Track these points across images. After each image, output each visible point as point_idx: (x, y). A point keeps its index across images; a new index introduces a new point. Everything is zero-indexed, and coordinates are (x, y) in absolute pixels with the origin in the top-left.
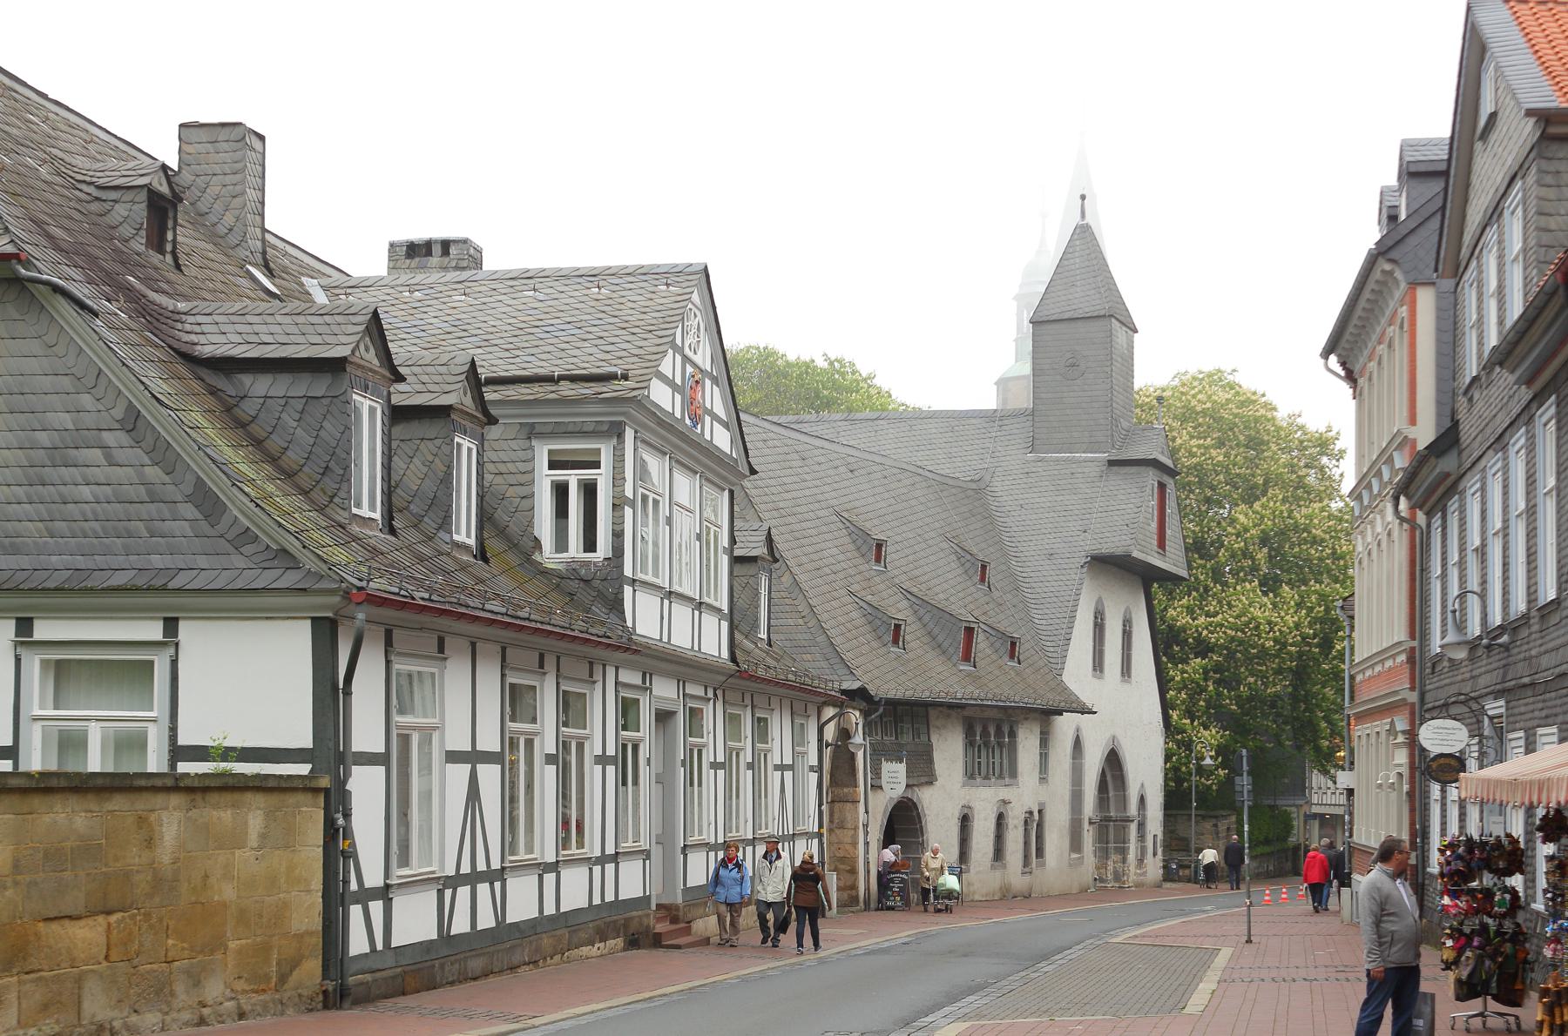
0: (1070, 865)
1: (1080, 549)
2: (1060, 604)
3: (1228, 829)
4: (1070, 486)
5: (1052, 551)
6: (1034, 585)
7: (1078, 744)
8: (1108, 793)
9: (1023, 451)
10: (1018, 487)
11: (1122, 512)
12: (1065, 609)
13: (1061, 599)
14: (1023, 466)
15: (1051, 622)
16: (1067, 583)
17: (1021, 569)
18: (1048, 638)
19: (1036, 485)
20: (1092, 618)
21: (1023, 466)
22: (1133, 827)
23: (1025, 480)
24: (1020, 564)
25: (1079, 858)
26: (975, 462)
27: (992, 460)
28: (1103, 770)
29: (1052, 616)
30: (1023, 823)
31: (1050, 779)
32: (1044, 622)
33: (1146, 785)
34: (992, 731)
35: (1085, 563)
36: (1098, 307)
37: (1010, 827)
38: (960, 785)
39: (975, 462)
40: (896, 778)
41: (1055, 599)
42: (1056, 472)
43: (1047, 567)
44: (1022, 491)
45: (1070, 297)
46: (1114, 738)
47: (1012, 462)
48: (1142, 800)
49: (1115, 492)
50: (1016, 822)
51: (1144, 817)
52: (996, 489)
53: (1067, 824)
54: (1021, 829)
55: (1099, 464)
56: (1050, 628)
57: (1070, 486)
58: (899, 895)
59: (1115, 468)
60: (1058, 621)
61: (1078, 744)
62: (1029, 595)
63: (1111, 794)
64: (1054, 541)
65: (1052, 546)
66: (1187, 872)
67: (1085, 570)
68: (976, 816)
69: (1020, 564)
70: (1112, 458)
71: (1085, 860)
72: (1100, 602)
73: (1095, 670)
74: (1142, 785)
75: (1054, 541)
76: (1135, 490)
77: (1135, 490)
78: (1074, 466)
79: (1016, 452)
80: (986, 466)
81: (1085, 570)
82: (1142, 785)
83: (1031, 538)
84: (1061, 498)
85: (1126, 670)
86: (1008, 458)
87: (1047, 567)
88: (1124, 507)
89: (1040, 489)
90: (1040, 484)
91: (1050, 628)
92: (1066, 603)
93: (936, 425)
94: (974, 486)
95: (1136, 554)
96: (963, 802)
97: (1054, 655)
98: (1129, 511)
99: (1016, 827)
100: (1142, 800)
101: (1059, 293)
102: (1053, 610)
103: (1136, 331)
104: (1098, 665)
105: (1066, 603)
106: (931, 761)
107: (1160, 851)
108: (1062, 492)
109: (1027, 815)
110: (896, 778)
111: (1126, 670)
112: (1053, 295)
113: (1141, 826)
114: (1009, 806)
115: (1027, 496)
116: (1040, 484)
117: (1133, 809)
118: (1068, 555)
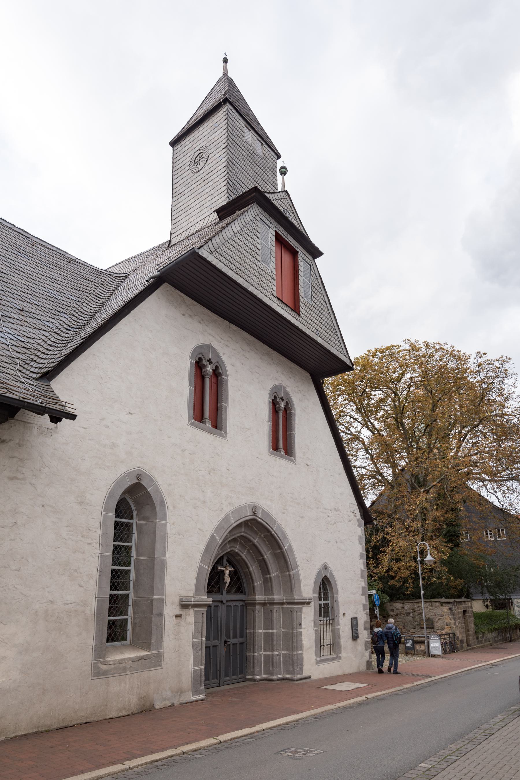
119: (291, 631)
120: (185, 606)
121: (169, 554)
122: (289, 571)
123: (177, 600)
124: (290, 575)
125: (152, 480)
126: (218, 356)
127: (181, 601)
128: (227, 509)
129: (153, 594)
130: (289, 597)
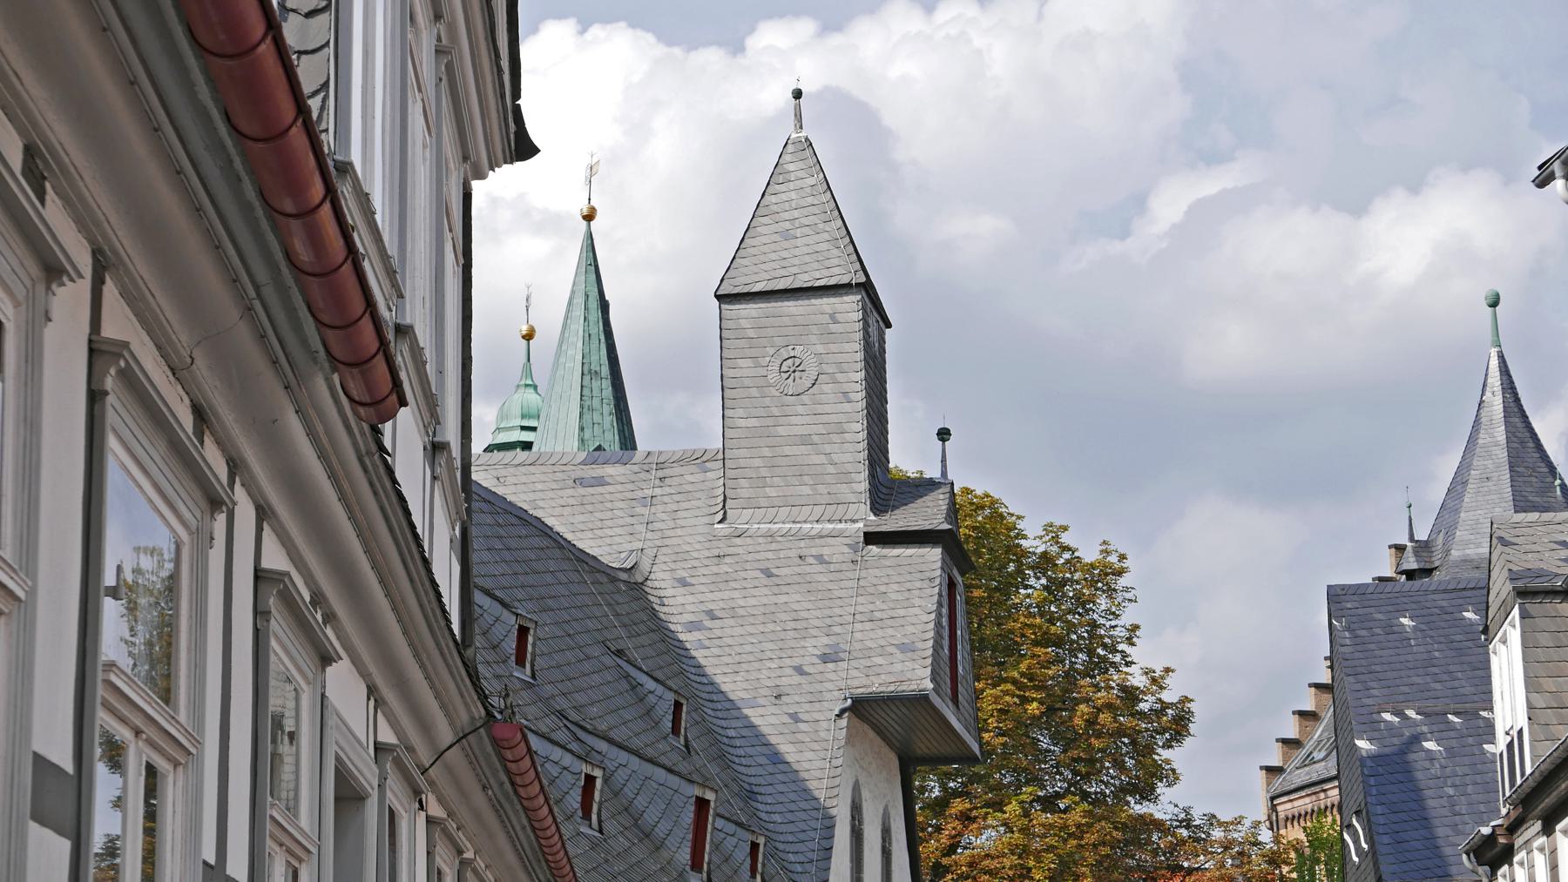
4: (798, 579)
9: (707, 520)
10: (703, 580)
11: (901, 621)
15: (790, 816)
17: (724, 723)
21: (707, 545)
23: (715, 569)
24: (719, 714)
26: (618, 539)
27: (649, 535)
29: (793, 807)
32: (777, 818)
35: (843, 711)
36: (836, 271)
39: (618, 539)
42: (770, 555)
44: (712, 587)
45: (785, 254)
47: (688, 539)
49: (883, 588)
52: (663, 585)
55: (848, 541)
56: (791, 828)
57: (798, 579)
64: (779, 672)
67: (844, 722)
69: (719, 714)
70: (870, 529)
76: (918, 584)
77: (918, 584)
78: (802, 544)
81: (844, 722)
84: (783, 599)
86: (679, 532)
88: (902, 612)
89: (745, 584)
90: (743, 574)
91: (791, 828)
98: (914, 620)
101: (766, 249)
108: (785, 589)
116: (743, 574)
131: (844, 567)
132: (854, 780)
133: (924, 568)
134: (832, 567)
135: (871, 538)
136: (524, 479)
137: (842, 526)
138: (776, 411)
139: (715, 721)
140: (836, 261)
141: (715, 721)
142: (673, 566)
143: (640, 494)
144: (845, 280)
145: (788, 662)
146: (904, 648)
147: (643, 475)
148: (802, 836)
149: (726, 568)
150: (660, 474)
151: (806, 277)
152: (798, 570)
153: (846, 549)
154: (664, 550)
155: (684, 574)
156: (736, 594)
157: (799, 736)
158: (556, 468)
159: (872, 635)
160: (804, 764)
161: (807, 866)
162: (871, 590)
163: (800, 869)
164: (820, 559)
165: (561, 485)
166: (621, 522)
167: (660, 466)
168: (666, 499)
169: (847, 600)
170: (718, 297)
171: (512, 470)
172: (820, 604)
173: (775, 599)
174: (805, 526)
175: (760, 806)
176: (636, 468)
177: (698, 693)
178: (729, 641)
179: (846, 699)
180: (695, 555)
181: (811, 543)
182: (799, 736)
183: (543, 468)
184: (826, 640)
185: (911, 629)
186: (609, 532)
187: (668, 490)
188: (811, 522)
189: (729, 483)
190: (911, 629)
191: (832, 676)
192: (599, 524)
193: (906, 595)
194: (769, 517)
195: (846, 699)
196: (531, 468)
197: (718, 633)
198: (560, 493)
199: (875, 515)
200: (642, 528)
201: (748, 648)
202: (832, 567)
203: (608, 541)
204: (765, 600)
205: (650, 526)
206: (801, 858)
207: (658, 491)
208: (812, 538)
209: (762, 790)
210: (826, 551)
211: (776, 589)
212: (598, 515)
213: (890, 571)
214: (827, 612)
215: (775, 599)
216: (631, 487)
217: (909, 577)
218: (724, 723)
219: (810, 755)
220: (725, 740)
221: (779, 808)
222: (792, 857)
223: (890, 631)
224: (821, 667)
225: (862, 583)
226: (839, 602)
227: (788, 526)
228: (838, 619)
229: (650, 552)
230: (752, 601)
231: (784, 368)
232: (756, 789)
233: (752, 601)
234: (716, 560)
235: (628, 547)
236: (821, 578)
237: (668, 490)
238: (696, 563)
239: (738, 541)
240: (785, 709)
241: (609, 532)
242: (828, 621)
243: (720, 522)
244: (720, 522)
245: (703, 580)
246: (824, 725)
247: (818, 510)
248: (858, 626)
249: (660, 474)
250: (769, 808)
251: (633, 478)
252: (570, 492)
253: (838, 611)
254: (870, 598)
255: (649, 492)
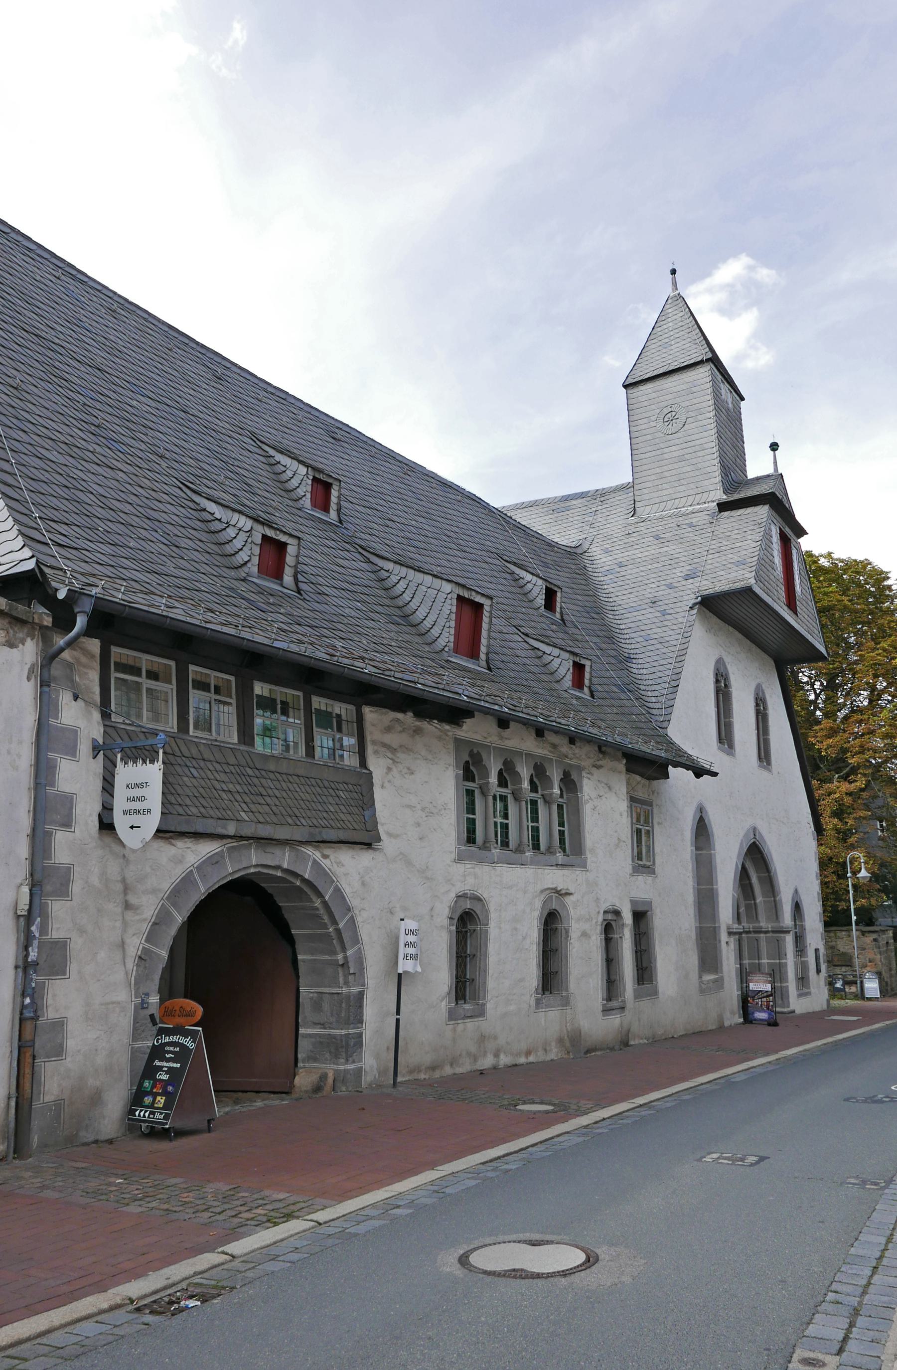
0: (702, 991)
1: (689, 592)
2: (665, 650)
3: (887, 943)
4: (676, 537)
5: (654, 600)
6: (632, 635)
7: (702, 829)
8: (754, 899)
9: (625, 517)
10: (618, 547)
11: (738, 549)
12: (671, 655)
13: (666, 645)
14: (623, 529)
15: (653, 670)
16: (674, 627)
18: (647, 688)
19: (637, 542)
20: (712, 679)
22: (789, 939)
23: (626, 541)
24: (617, 617)
25: (715, 981)
27: (592, 530)
28: (744, 868)
29: (655, 664)
30: (599, 929)
31: (658, 869)
32: (644, 671)
33: (800, 891)
34: (525, 772)
37: (574, 934)
38: (453, 856)
40: (141, 799)
41: (659, 646)
42: (660, 528)
43: (650, 616)
44: (623, 550)
46: (755, 829)
48: (797, 908)
49: (728, 534)
50: (586, 926)
51: (803, 928)
52: (594, 554)
53: (693, 934)
54: (597, 940)
55: (709, 513)
56: (652, 676)
57: (676, 537)
58: (165, 1093)
59: (726, 514)
60: (661, 668)
61: (702, 829)
62: (626, 646)
63: (759, 899)
64: (657, 589)
65: (656, 594)
66: (853, 989)
67: (695, 611)
68: (493, 916)
69: (617, 617)
71: (726, 980)
72: (720, 662)
73: (720, 740)
74: (796, 891)
75: (657, 589)
76: (752, 528)
78: (680, 519)
79: (619, 519)
80: (585, 536)
81: (695, 611)
82: (796, 891)
83: (631, 591)
85: (764, 755)
86: (608, 526)
87: (650, 616)
90: (643, 541)
91: (652, 676)
92: (672, 649)
93: (536, 512)
94: (569, 549)
95: (757, 589)
96: (460, 888)
97: (658, 706)
99: (585, 934)
100: (797, 908)
102: (656, 658)
103: (742, 399)
104: (725, 737)
105: (672, 649)
106: (366, 802)
107: (823, 967)
108: (666, 544)
109: (610, 917)
110: (141, 799)
111: (764, 755)
112: (646, 358)
113: (799, 940)
114: (569, 900)
115: (627, 554)
116: (643, 541)
117: (787, 919)
118: (675, 600)
119: (778, 961)
120: (730, 934)
121: (719, 883)
122: (774, 897)
123: (725, 928)
124: (775, 901)
125: (706, 812)
126: (726, 668)
127: (728, 928)
128: (742, 834)
129: (715, 923)
130: (775, 924)
131: (705, 526)
132: (717, 657)
133: (755, 518)
134: (697, 528)
135: (723, 507)
136: (525, 514)
137: (706, 505)
138: (662, 445)
139: (613, 621)
140: (695, 351)
141: (613, 621)
142: (602, 543)
143: (590, 511)
144: (699, 359)
145: (664, 583)
146: (738, 563)
147: (593, 501)
148: (659, 681)
149: (633, 539)
150: (602, 499)
151: (676, 363)
152: (676, 533)
153: (707, 517)
154: (598, 536)
155: (608, 546)
156: (637, 551)
157: (666, 623)
158: (544, 506)
159: (719, 560)
160: (666, 638)
161: (660, 699)
162: (722, 536)
163: (654, 701)
164: (691, 525)
165: (546, 514)
166: (576, 526)
167: (602, 495)
168: (603, 511)
169: (705, 544)
170: (626, 386)
171: (520, 511)
172: (688, 549)
173: (660, 550)
174: (683, 509)
175: (633, 665)
176: (589, 499)
177: (604, 607)
178: (628, 577)
179: (697, 598)
180: (616, 535)
181: (686, 517)
182: (666, 623)
183: (537, 507)
184: (689, 567)
185: (745, 552)
186: (569, 533)
187: (606, 506)
188: (686, 507)
189: (637, 493)
190: (745, 552)
191: (691, 586)
192: (564, 530)
193: (744, 534)
194: (662, 508)
195: (697, 598)
196: (531, 509)
197: (623, 574)
198: (545, 518)
199: (726, 495)
200: (588, 527)
201: (640, 579)
202: (697, 528)
203: (567, 537)
204: (653, 552)
205: (592, 526)
206: (656, 694)
207: (600, 508)
208: (687, 515)
209: (637, 656)
210: (694, 520)
211: (661, 545)
212: (565, 525)
213: (734, 524)
214: (693, 552)
215: (660, 550)
216: (585, 508)
217: (746, 525)
218: (619, 622)
219: (671, 633)
220: (618, 631)
221: (646, 666)
222: (650, 694)
223: (731, 556)
224: (684, 583)
225: (715, 533)
226: (700, 546)
227: (672, 511)
228: (698, 555)
229: (590, 539)
230: (647, 554)
231: (666, 419)
232: (632, 656)
233: (647, 554)
234: (627, 536)
235: (579, 538)
236: (690, 535)
237: (606, 506)
238: (615, 540)
239: (642, 524)
240: (658, 609)
241: (569, 533)
242: (692, 557)
243: (632, 516)
244: (632, 516)
245: (618, 547)
246: (682, 614)
247: (691, 499)
248: (710, 556)
249: (602, 499)
250: (639, 666)
251: (587, 503)
252: (551, 516)
253: (698, 551)
254: (720, 540)
255: (595, 509)
